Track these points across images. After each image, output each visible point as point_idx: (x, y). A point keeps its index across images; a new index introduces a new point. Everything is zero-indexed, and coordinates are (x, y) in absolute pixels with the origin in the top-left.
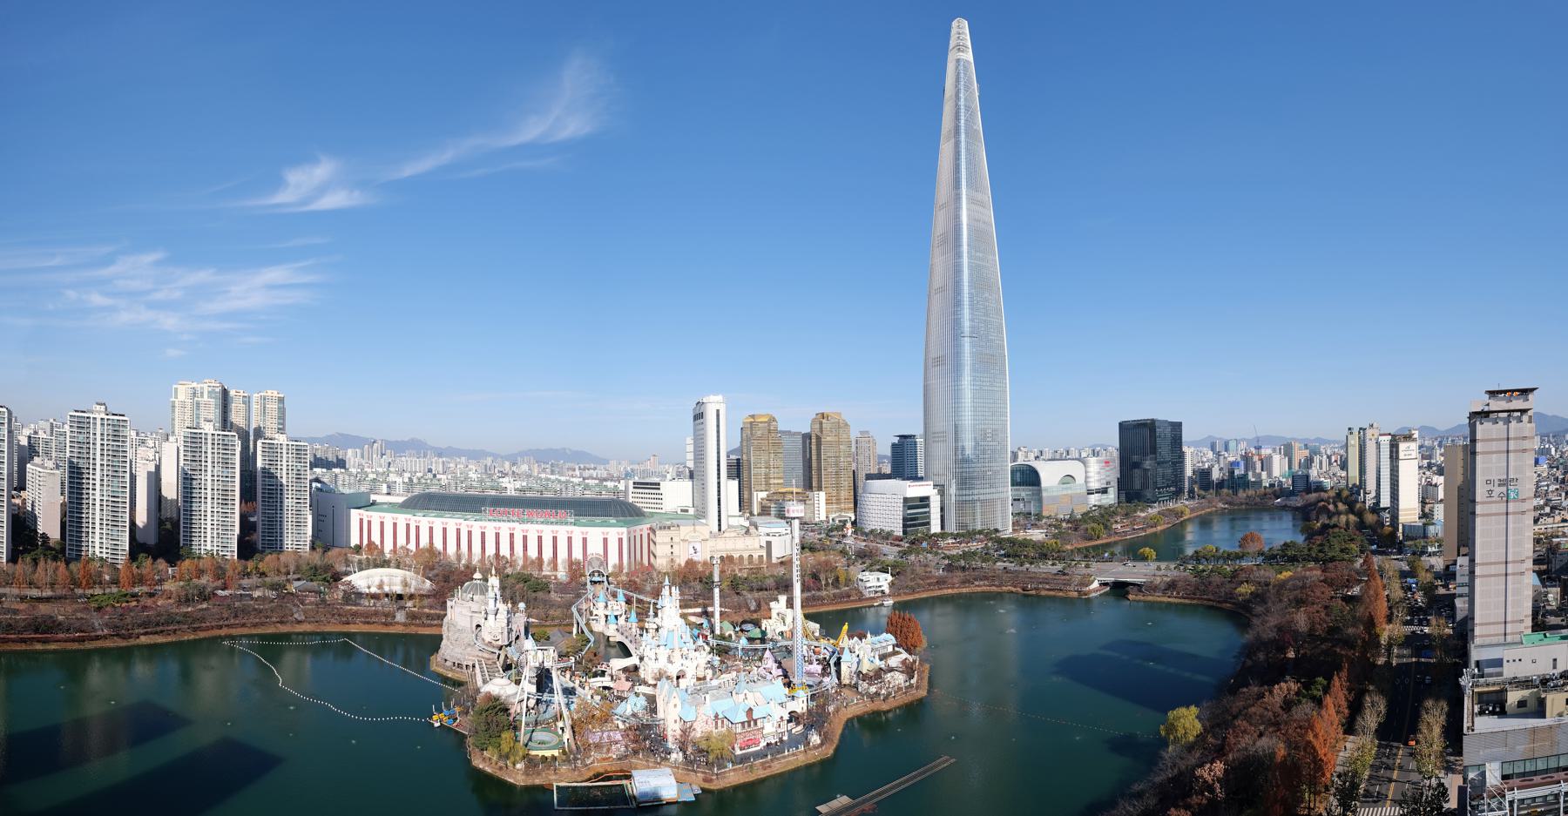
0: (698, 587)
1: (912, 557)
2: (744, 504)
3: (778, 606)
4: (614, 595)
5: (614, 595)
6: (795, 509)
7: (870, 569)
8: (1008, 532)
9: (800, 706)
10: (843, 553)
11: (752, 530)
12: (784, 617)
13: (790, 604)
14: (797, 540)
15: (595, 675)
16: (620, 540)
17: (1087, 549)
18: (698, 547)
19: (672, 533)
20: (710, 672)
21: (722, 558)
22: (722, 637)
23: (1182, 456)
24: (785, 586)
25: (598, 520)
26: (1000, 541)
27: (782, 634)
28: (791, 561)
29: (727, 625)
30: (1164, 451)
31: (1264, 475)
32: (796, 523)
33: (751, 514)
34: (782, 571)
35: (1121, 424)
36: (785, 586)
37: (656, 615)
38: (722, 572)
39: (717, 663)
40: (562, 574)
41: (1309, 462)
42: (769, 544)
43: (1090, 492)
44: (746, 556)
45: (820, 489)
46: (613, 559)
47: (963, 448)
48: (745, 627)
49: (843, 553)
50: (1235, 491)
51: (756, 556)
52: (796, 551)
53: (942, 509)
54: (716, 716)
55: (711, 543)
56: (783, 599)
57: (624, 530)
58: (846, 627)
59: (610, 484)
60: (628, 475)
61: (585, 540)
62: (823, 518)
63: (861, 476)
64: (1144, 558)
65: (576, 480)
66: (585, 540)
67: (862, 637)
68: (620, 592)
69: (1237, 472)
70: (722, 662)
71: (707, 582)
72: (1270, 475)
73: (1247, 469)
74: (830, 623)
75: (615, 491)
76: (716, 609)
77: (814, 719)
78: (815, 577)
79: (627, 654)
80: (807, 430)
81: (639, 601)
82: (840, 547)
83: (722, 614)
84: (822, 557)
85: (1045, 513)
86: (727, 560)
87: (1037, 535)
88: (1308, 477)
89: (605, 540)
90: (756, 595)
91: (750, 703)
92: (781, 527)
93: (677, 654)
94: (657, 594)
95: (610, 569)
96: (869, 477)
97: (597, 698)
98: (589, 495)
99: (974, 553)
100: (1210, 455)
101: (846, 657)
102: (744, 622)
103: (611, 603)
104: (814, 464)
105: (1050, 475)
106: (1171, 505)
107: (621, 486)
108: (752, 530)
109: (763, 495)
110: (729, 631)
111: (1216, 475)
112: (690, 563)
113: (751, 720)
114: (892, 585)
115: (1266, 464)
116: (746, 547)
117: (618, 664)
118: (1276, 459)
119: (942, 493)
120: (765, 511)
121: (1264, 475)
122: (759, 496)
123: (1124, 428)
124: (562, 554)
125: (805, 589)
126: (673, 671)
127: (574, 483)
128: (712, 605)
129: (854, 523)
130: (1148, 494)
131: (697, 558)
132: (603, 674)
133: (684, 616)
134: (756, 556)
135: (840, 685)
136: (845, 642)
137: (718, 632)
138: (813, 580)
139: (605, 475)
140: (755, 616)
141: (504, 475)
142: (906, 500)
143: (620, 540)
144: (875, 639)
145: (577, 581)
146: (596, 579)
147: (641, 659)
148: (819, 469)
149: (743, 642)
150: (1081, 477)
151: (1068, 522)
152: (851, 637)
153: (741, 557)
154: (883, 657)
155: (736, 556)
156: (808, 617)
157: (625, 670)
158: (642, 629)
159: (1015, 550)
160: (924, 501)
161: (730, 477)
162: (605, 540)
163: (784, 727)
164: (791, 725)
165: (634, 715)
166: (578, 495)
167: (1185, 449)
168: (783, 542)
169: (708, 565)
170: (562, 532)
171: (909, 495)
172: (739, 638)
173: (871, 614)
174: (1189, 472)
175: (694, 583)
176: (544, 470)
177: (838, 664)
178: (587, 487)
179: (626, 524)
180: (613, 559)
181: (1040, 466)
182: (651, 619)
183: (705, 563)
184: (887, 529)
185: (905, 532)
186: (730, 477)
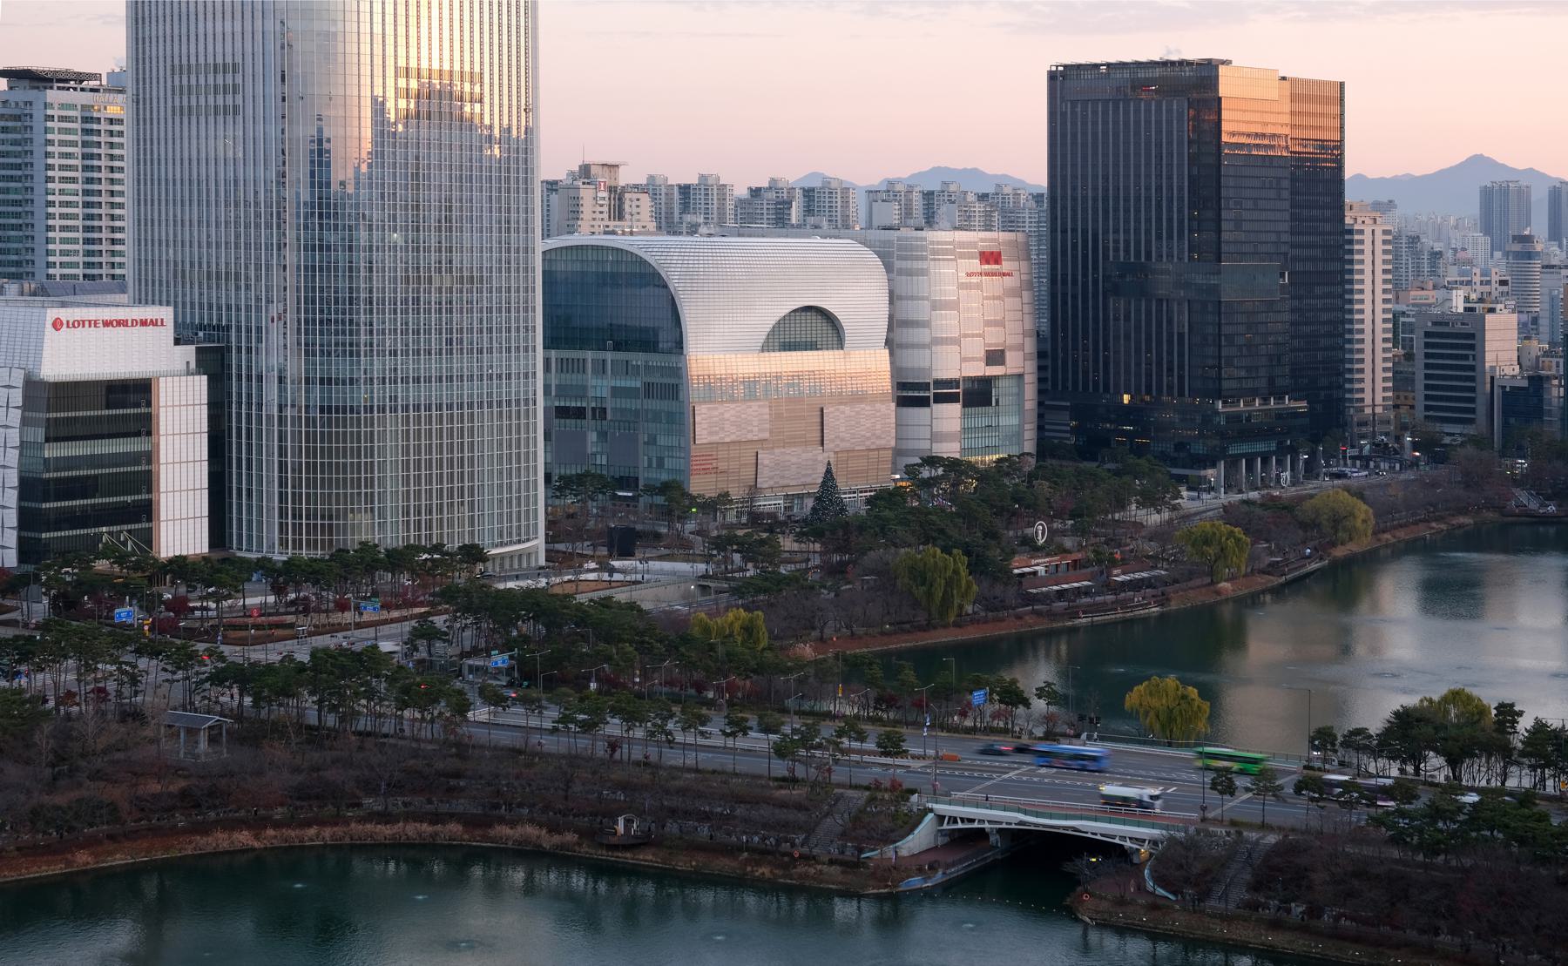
35: (1077, 95)
47: (320, 156)
119: (216, 363)
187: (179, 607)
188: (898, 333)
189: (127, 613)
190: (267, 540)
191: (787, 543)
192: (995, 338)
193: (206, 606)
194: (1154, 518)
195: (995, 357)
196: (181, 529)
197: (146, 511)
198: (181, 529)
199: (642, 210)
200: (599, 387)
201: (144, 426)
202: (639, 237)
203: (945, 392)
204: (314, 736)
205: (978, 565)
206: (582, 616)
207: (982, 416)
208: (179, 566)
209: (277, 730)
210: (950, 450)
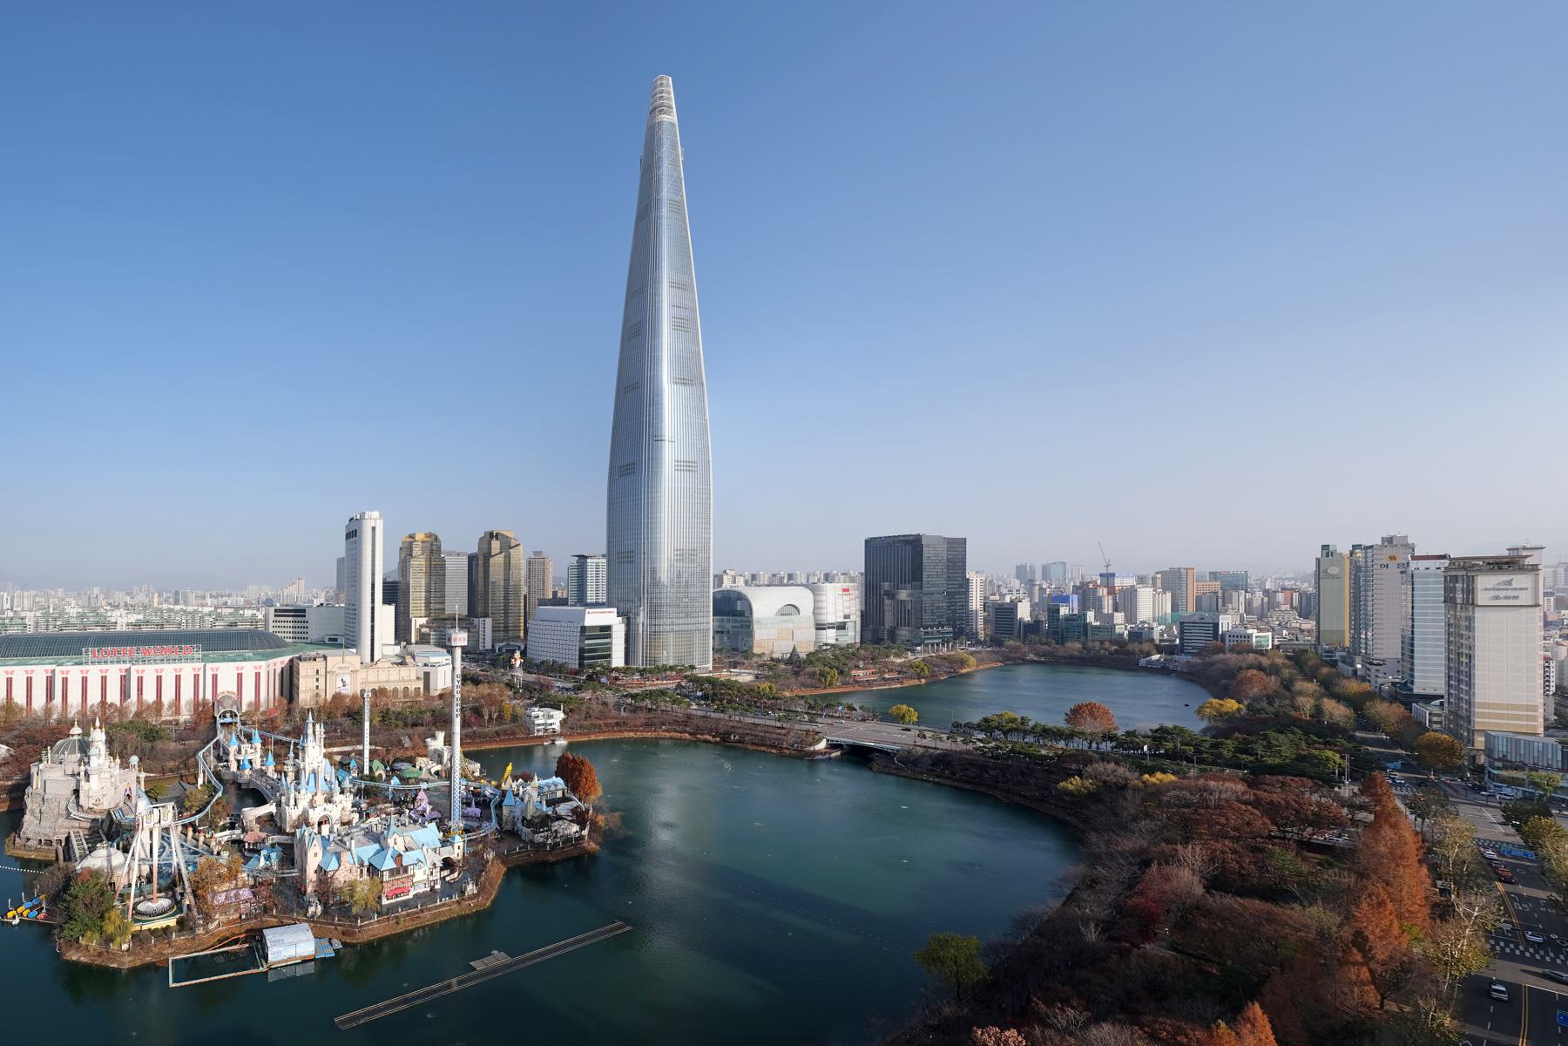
0: (347, 722)
1: (587, 695)
2: (402, 632)
3: (437, 743)
4: (249, 738)
5: (249, 738)
6: (460, 638)
7: (542, 703)
8: (705, 666)
9: (457, 850)
10: (510, 685)
11: (409, 659)
12: (446, 756)
13: (448, 741)
14: (458, 671)
15: (223, 829)
16: (258, 675)
17: (814, 697)
18: (347, 678)
19: (320, 664)
20: (356, 816)
21: (374, 691)
22: (372, 777)
23: (966, 583)
24: (444, 722)
25: (232, 653)
26: (696, 680)
27: (437, 773)
28: (451, 694)
29: (377, 763)
30: (933, 574)
31: (1119, 618)
32: (458, 652)
33: (409, 643)
34: (438, 704)
36: (444, 722)
37: (296, 757)
38: (374, 705)
39: (364, 806)
40: (185, 716)
41: (1219, 602)
42: (427, 675)
43: (820, 627)
44: (401, 687)
45: (486, 616)
46: (248, 696)
48: (398, 765)
49: (510, 685)
50: (1063, 639)
51: (412, 688)
52: (458, 680)
53: (627, 641)
54: (362, 865)
55: (362, 675)
56: (441, 735)
57: (263, 663)
58: (510, 768)
59: (248, 613)
60: (269, 603)
61: (215, 677)
62: (488, 646)
63: (534, 600)
64: (900, 718)
65: (206, 610)
66: (215, 677)
67: (528, 779)
68: (256, 734)
69: (1064, 611)
70: (370, 805)
71: (355, 715)
72: (1131, 617)
73: (1084, 607)
74: (492, 762)
75: (253, 620)
76: (367, 747)
77: (474, 865)
78: (477, 711)
79: (260, 800)
80: (474, 550)
81: (277, 742)
82: (506, 679)
83: (372, 752)
84: (484, 689)
85: (756, 650)
86: (379, 693)
87: (745, 677)
88: (1216, 625)
89: (240, 676)
90: (410, 731)
91: (400, 848)
92: (441, 658)
93: (320, 799)
94: (299, 732)
95: (244, 709)
96: (543, 602)
97: (225, 854)
98: (220, 626)
99: (663, 693)
100: (1016, 584)
101: (509, 800)
102: (397, 760)
103: (245, 746)
104: (480, 588)
105: (765, 605)
106: (944, 651)
107: (260, 616)
108: (409, 659)
109: (424, 621)
110: (380, 771)
111: (1024, 612)
112: (338, 697)
113: (401, 869)
114: (563, 723)
115: (1127, 601)
116: (404, 679)
117: (252, 814)
118: (1145, 596)
120: (423, 639)
121: (1119, 618)
122: (418, 621)
123: (876, 549)
124: (187, 695)
125: (464, 724)
126: (315, 816)
127: (204, 611)
128: (361, 742)
129: (523, 654)
130: (904, 633)
131: (347, 691)
132: (232, 827)
133: (325, 756)
134: (412, 688)
135: (500, 831)
136: (509, 784)
137: (367, 772)
138: (473, 714)
139: (241, 601)
140: (409, 753)
141: (117, 607)
142: (584, 629)
143: (258, 675)
144: (543, 782)
145: (207, 721)
146: (228, 720)
147: (279, 805)
148: (486, 593)
149: (395, 781)
150: (802, 613)
151: (789, 662)
152: (515, 778)
153: (395, 691)
154: (551, 803)
155: (390, 687)
156: (466, 755)
157: (259, 819)
158: (279, 772)
159: (714, 692)
160: (606, 630)
161: (386, 601)
162: (240, 676)
163: (437, 875)
164: (446, 873)
165: (267, 869)
166: (207, 626)
167: (970, 574)
168: (445, 673)
169: (358, 699)
170: (188, 670)
171: (587, 624)
172: (389, 778)
173: (539, 753)
174: (976, 603)
175: (342, 719)
176: (166, 601)
177: (499, 806)
178: (219, 617)
179: (267, 657)
180: (248, 696)
181: (752, 594)
182: (290, 762)
183: (354, 697)
184: (560, 661)
185: (581, 665)
186: (386, 601)
187: (616, 679)
188: (816, 610)
189: (603, 680)
190: (639, 664)
191: (782, 666)
192: (847, 612)
193: (625, 680)
194: (899, 661)
195: (847, 617)
196: (618, 660)
197: (609, 656)
198: (618, 660)
199: (740, 581)
200: (728, 626)
201: (609, 636)
202: (740, 585)
203: (831, 626)
204: (650, 710)
205: (841, 673)
206: (723, 684)
207: (842, 632)
208: (617, 669)
209: (641, 708)
210: (832, 641)
